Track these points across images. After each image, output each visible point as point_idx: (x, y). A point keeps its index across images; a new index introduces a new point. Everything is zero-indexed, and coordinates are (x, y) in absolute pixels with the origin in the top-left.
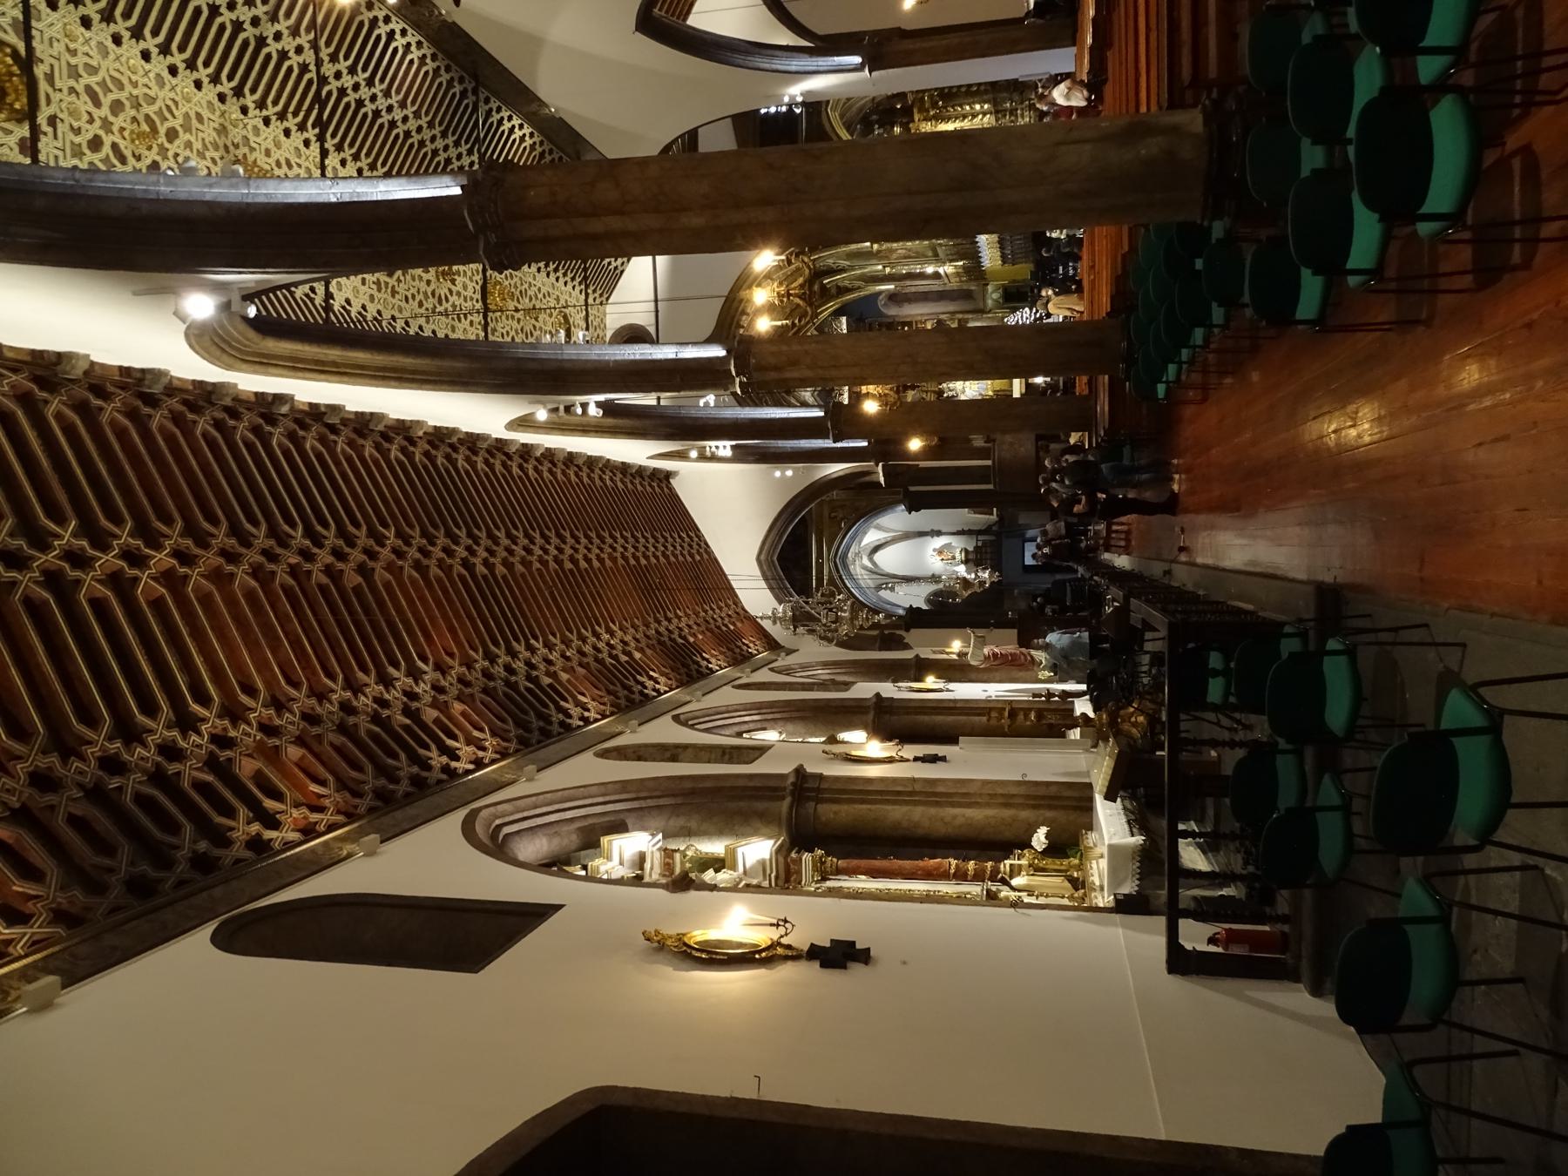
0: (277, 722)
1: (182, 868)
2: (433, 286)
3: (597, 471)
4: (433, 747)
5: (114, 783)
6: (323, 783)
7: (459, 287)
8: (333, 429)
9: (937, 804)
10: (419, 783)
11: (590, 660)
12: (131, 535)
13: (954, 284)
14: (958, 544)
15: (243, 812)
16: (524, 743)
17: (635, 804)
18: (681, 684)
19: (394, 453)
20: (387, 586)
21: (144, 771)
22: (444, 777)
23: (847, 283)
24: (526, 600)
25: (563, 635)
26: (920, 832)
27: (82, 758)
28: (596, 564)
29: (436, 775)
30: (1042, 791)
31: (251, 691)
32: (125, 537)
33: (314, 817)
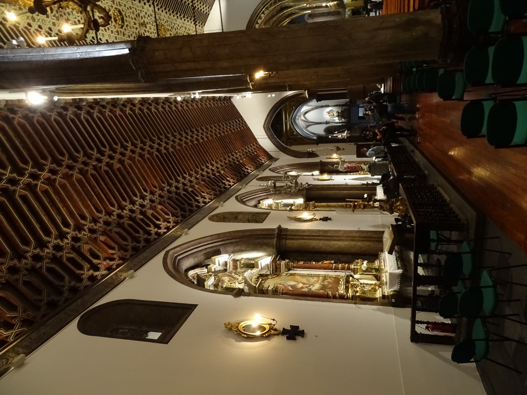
0: (95, 227)
1: (66, 294)
2: (138, 30)
3: (204, 102)
4: (152, 225)
5: (39, 265)
6: (112, 248)
7: (148, 29)
8: (104, 107)
9: (328, 240)
10: (147, 241)
11: (205, 178)
12: (32, 168)
13: (333, 9)
14: (335, 110)
15: (86, 266)
16: (184, 217)
17: (223, 243)
18: (238, 181)
19: (128, 111)
20: (130, 166)
21: (49, 258)
22: (156, 237)
23: (293, 11)
24: (181, 159)
25: (195, 170)
26: (322, 250)
27: (26, 258)
28: (206, 139)
29: (154, 236)
30: (365, 235)
31: (84, 218)
32: (30, 169)
33: (111, 263)
